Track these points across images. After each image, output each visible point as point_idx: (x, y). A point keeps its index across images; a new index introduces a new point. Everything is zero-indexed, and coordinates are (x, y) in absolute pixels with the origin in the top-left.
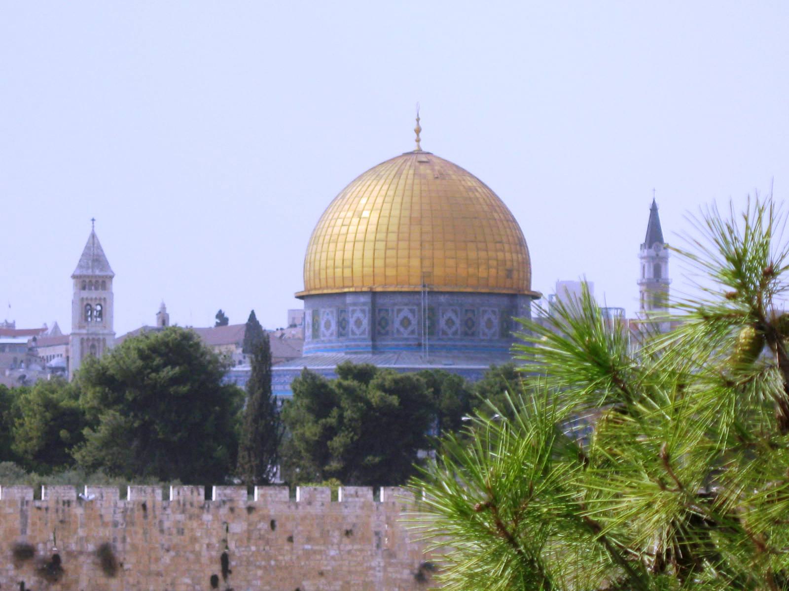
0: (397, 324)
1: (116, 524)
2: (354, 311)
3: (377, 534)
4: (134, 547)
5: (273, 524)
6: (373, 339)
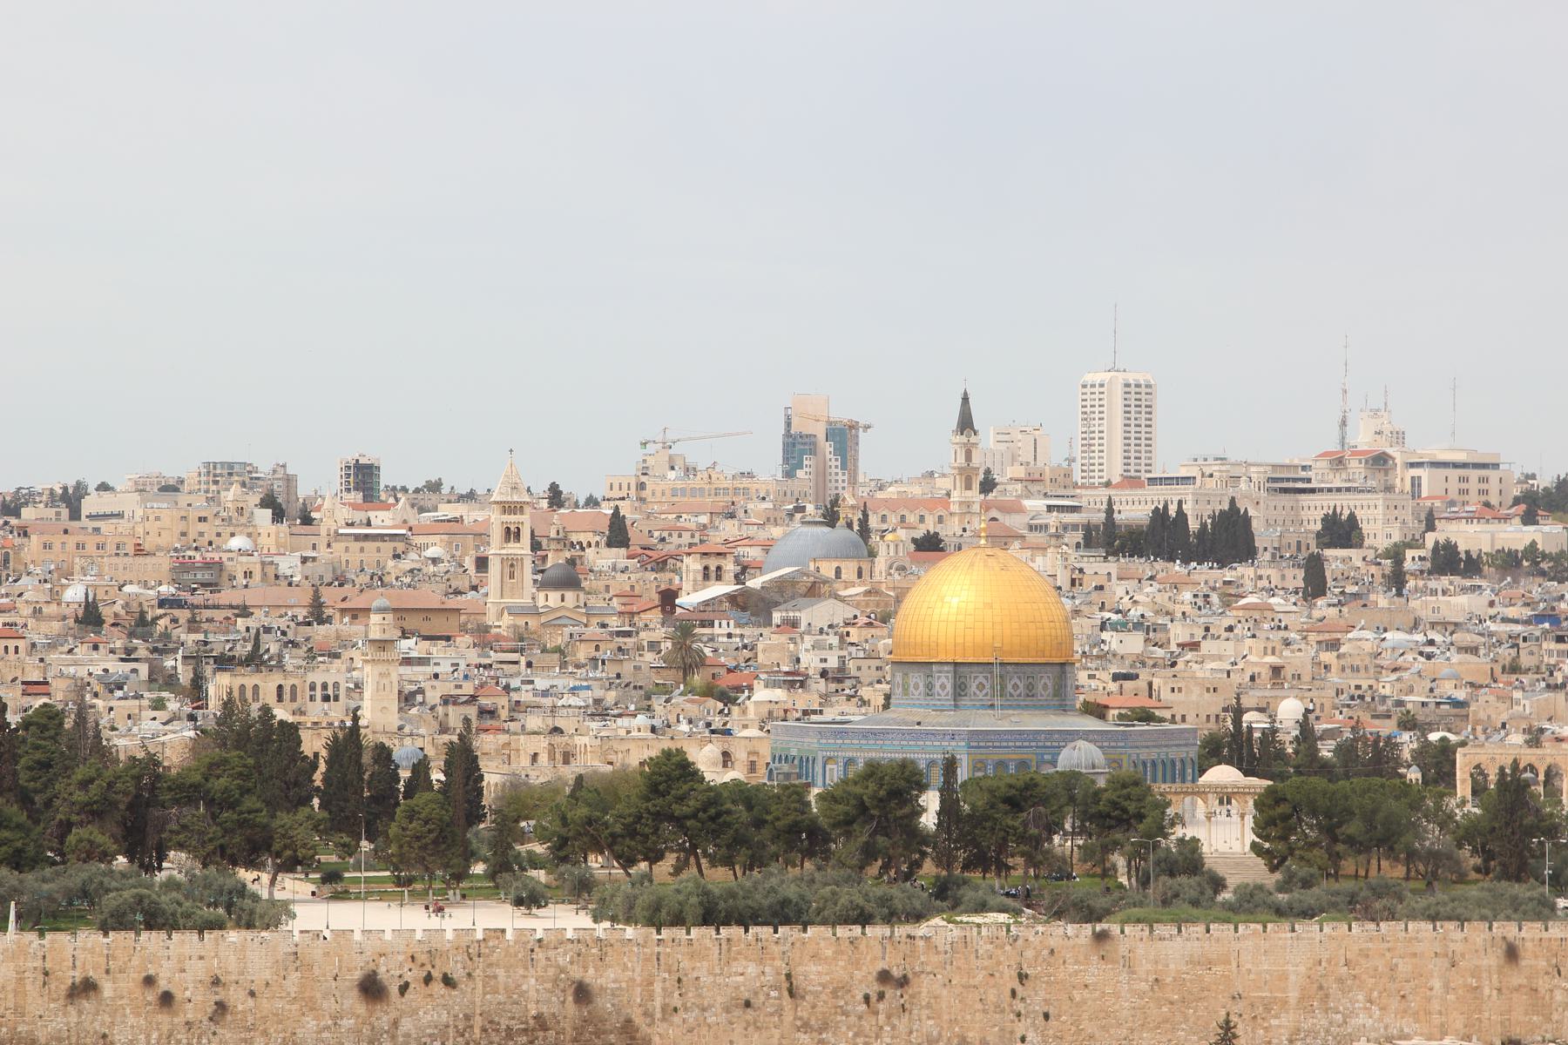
0: (974, 688)
1: (946, 953)
2: (939, 678)
3: (1123, 957)
4: (959, 968)
5: (1052, 952)
6: (955, 700)
